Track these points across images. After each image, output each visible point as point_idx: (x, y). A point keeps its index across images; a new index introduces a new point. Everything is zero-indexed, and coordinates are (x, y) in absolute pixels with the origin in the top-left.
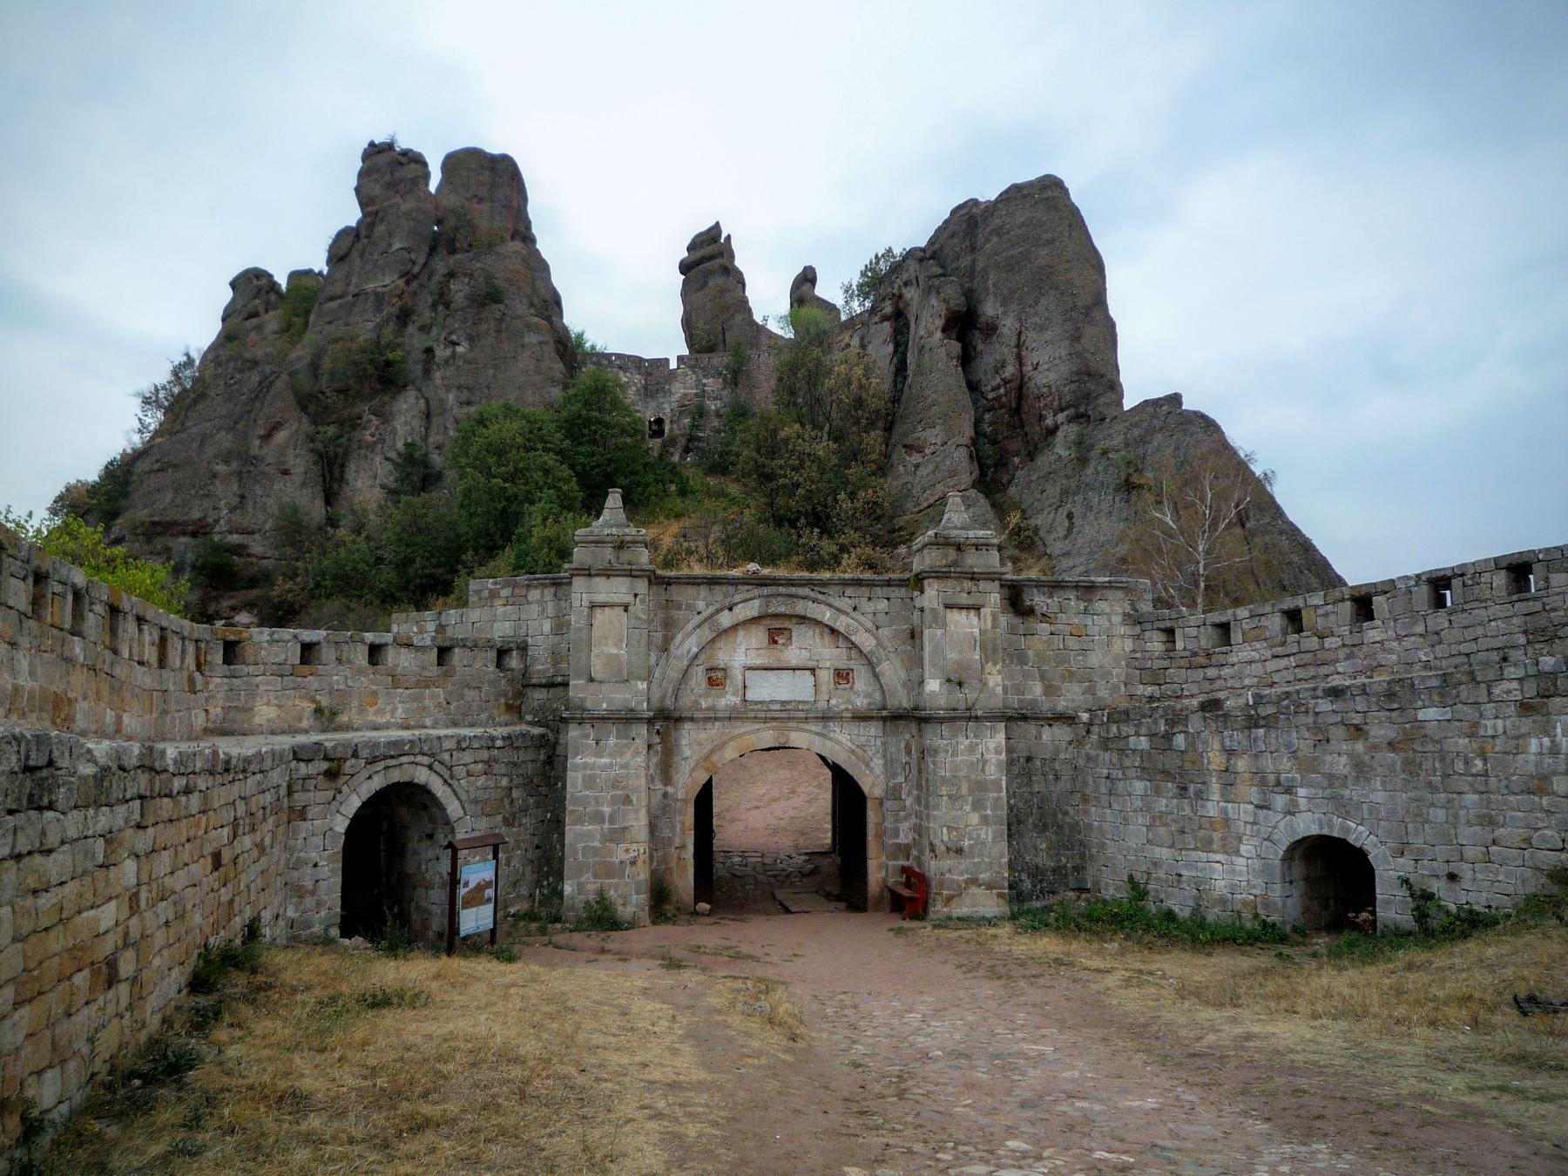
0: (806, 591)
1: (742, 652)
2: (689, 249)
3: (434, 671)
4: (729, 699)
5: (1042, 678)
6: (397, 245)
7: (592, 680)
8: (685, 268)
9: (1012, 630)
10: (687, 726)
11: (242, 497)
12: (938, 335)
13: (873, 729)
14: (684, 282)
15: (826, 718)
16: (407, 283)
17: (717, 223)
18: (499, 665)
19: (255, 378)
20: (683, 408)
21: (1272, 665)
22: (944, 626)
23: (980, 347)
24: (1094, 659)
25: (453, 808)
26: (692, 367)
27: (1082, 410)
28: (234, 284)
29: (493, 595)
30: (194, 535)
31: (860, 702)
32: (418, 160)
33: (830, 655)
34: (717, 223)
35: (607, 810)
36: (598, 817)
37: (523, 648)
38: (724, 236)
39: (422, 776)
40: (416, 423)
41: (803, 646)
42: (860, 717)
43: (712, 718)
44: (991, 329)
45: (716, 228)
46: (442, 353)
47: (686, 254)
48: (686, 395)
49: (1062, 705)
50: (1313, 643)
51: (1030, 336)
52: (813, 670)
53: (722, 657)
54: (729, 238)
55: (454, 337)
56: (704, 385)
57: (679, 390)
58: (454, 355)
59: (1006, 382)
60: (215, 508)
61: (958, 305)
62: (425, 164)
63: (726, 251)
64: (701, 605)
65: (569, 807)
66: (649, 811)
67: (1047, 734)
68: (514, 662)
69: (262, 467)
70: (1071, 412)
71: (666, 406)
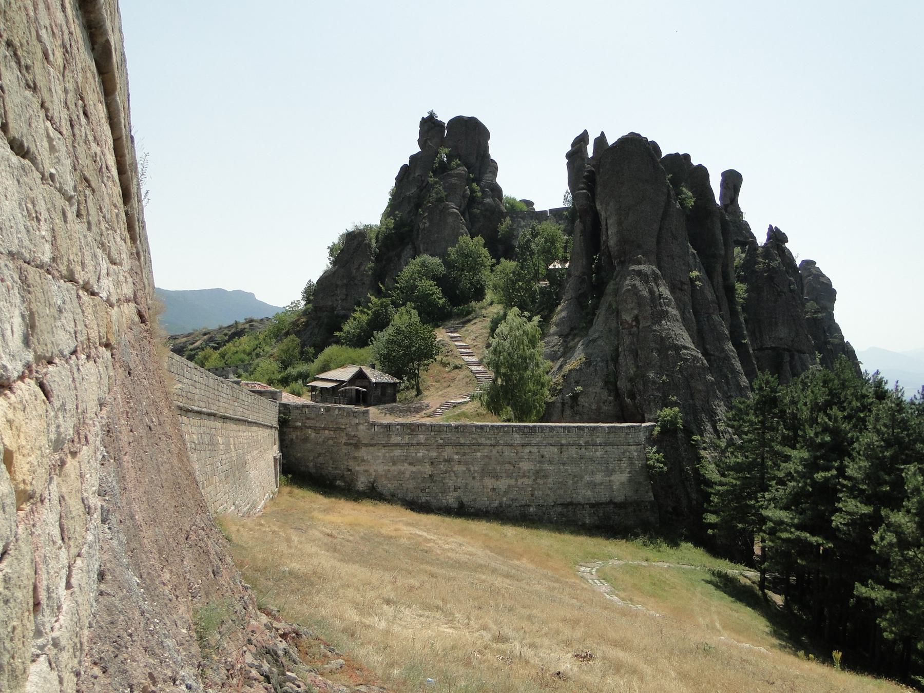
2: (573, 145)
6: (417, 174)
8: (569, 156)
11: (347, 295)
14: (568, 164)
16: (421, 191)
17: (586, 131)
19: (356, 243)
26: (555, 216)
27: (622, 259)
46: (421, 226)
47: (570, 148)
54: (602, 132)
60: (336, 300)
69: (356, 282)
70: (618, 260)
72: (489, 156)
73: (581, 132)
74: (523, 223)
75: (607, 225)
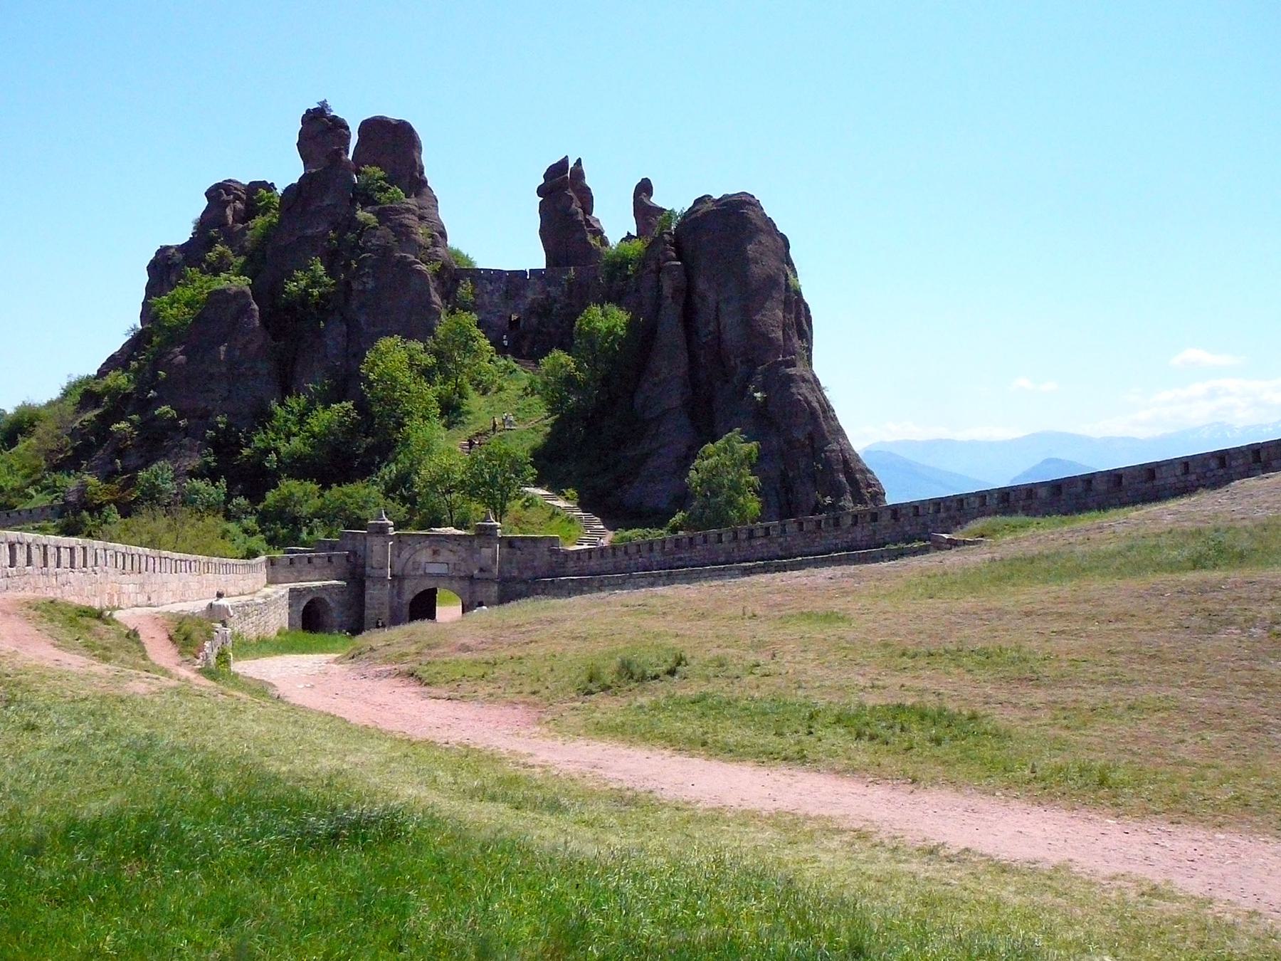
0: (442, 539)
1: (424, 556)
2: (546, 176)
3: (327, 564)
4: (421, 572)
5: (518, 568)
7: (372, 568)
8: (541, 191)
9: (508, 553)
10: (406, 581)
12: (670, 300)
13: (467, 583)
15: (452, 578)
17: (567, 157)
18: (348, 561)
20: (531, 311)
21: (575, 569)
22: (480, 553)
23: (699, 306)
24: (535, 564)
25: (332, 605)
28: (208, 194)
29: (346, 536)
30: (201, 418)
31: (462, 574)
32: (339, 126)
33: (453, 558)
34: (567, 157)
35: (376, 606)
36: (374, 608)
37: (355, 553)
38: (571, 165)
39: (324, 595)
40: (340, 339)
41: (445, 555)
42: (461, 578)
43: (415, 577)
44: (703, 298)
45: (564, 162)
47: (543, 181)
48: (534, 300)
49: (525, 576)
50: (581, 563)
51: (722, 306)
52: (448, 564)
53: (418, 559)
54: (579, 162)
55: (365, 280)
56: (548, 292)
57: (530, 295)
58: (363, 291)
59: (710, 333)
61: (679, 283)
62: (347, 128)
63: (578, 173)
64: (410, 543)
65: (366, 605)
66: (391, 608)
67: (518, 587)
68: (352, 559)
71: (521, 306)
72: (425, 182)
73: (556, 160)
74: (490, 288)
75: (718, 309)
